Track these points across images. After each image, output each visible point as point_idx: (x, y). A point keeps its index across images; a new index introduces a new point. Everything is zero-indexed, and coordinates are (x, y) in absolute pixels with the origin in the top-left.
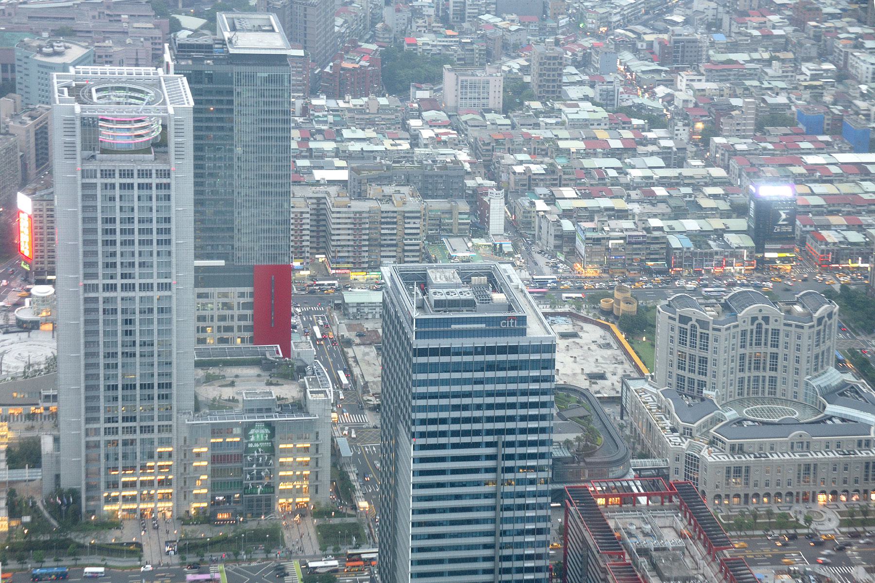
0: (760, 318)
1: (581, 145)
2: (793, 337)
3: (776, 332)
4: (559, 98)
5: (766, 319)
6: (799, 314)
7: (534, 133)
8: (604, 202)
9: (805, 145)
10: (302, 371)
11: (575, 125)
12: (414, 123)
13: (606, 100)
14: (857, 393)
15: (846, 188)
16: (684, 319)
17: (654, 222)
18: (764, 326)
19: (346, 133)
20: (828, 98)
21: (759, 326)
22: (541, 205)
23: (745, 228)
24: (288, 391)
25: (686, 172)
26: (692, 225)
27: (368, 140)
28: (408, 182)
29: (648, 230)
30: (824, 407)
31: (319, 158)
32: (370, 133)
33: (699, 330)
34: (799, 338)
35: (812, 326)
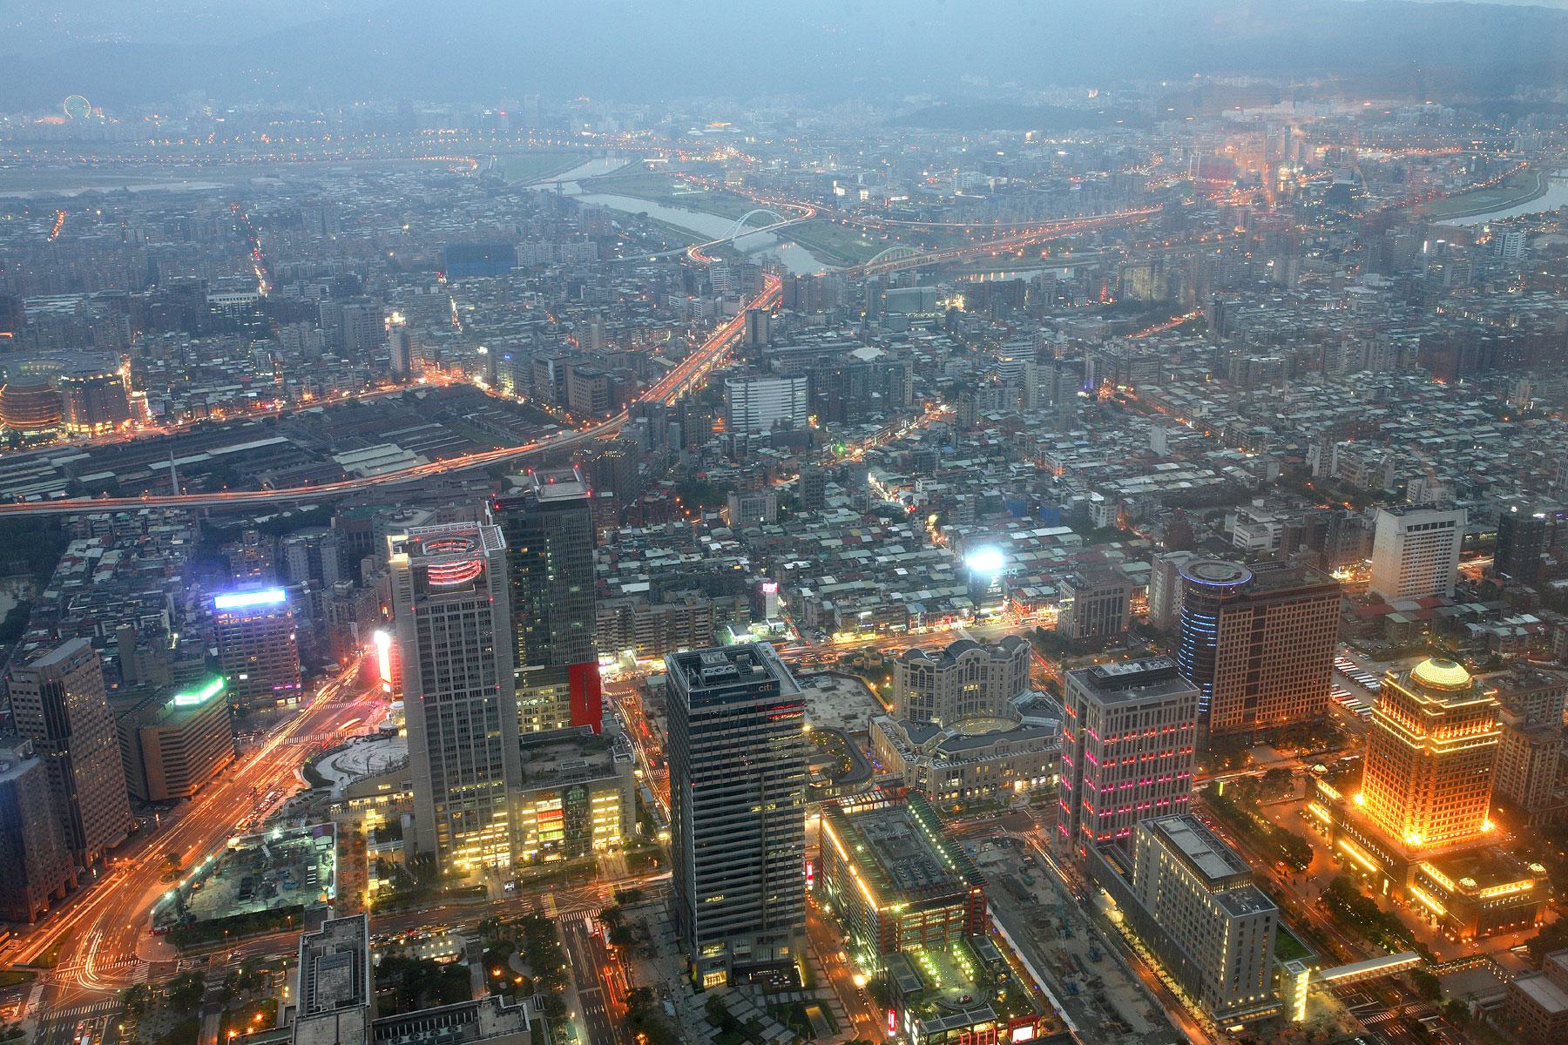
1: (840, 542)
4: (822, 508)
5: (977, 660)
7: (802, 537)
8: (859, 584)
9: (1012, 525)
10: (610, 742)
11: (835, 527)
12: (704, 539)
13: (860, 505)
15: (1042, 555)
16: (914, 667)
17: (896, 595)
19: (649, 553)
20: (1029, 489)
22: (806, 592)
24: (598, 759)
25: (921, 554)
26: (925, 594)
27: (667, 556)
28: (698, 586)
29: (891, 602)
31: (628, 577)
32: (668, 551)
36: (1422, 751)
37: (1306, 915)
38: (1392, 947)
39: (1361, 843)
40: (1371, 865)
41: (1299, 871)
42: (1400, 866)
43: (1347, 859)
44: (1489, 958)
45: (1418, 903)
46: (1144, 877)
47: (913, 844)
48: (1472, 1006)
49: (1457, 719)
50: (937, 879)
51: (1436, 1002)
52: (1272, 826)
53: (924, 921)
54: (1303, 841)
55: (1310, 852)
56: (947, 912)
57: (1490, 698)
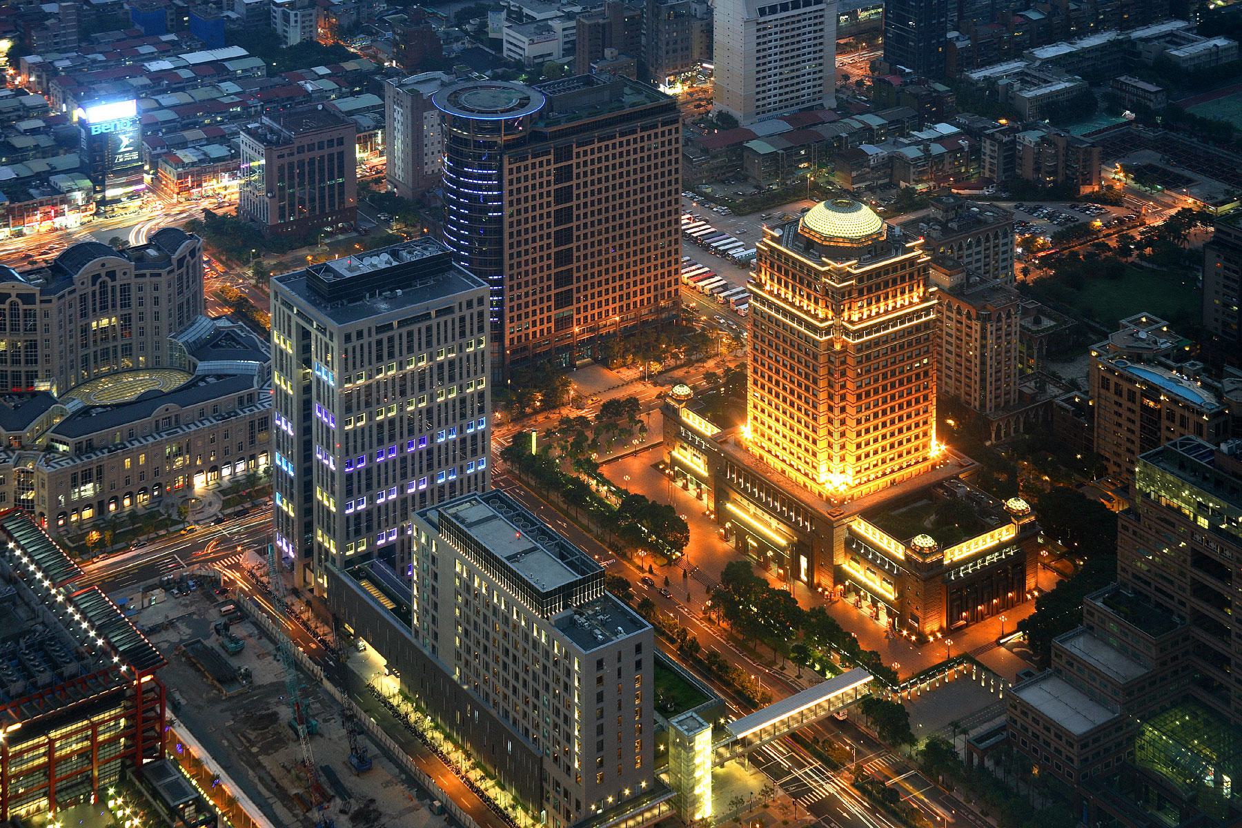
0: (103, 275)
2: (148, 289)
3: (125, 289)
5: (112, 275)
6: (155, 258)
9: (146, 49)
14: (234, 340)
15: (201, 94)
18: (110, 284)
21: (103, 284)
23: (77, 165)
30: (195, 367)
33: (22, 307)
34: (156, 289)
35: (172, 271)
36: (831, 344)
37: (692, 633)
38: (827, 666)
39: (758, 502)
40: (775, 532)
41: (671, 563)
42: (816, 531)
43: (740, 532)
44: (972, 661)
45: (856, 588)
46: (433, 606)
47: (21, 612)
48: (959, 743)
49: (872, 287)
50: (71, 668)
51: (906, 748)
52: (619, 492)
53: (50, 753)
54: (670, 509)
55: (684, 528)
56: (94, 726)
57: (917, 250)
